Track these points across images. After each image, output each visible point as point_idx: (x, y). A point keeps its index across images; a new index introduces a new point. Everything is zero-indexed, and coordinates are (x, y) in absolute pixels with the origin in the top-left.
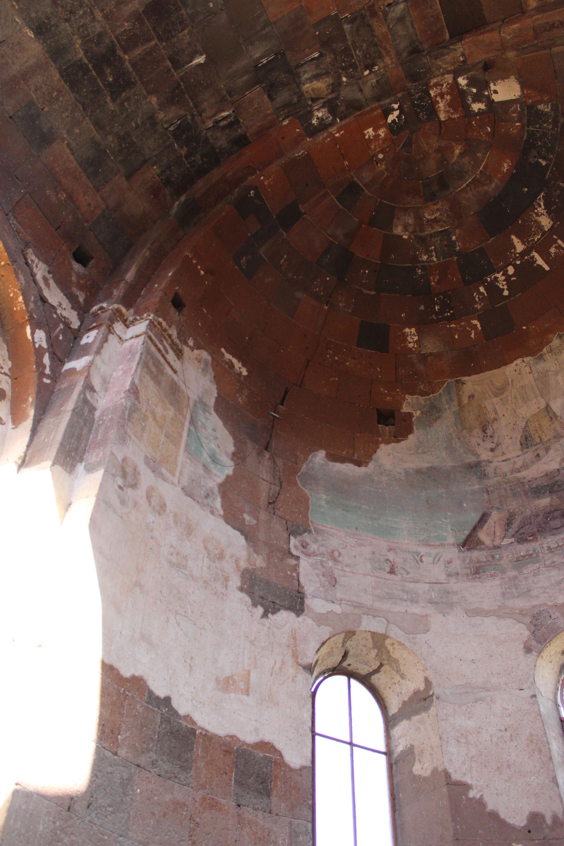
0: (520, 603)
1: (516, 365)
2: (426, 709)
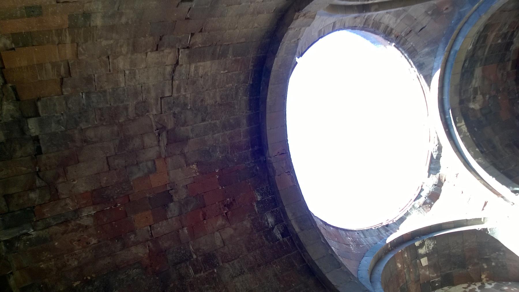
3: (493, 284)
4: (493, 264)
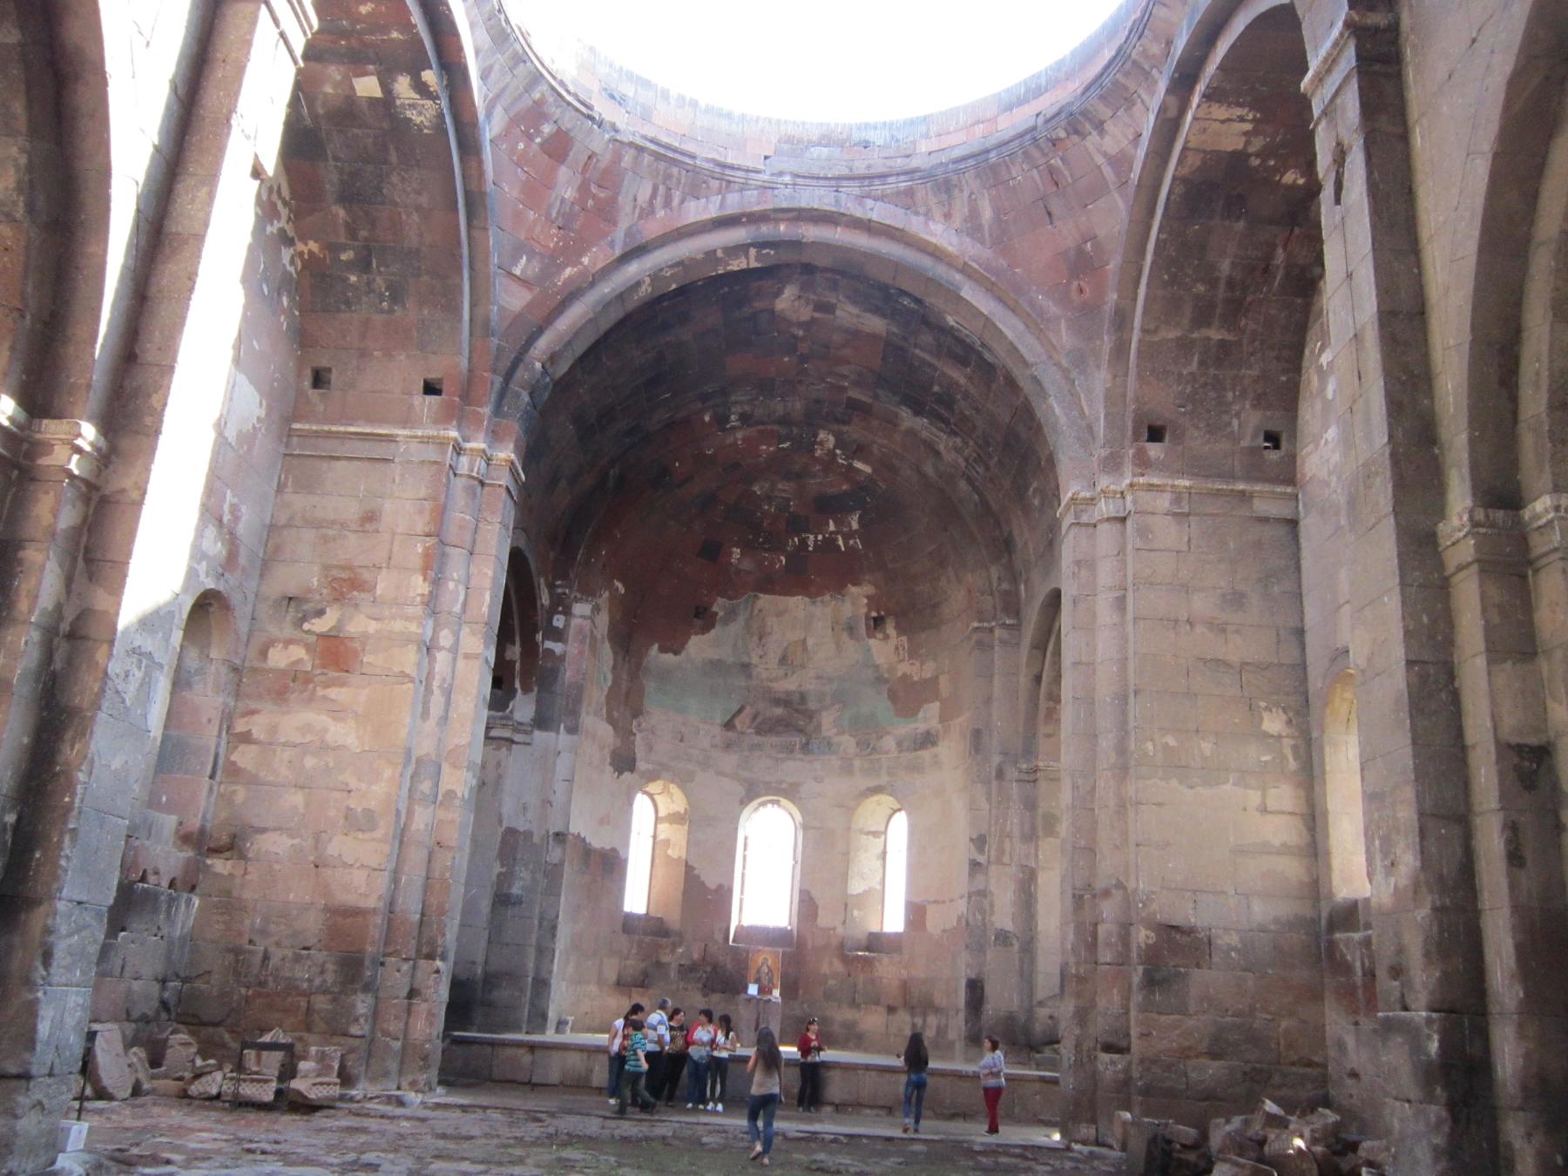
0: (746, 774)
2: (682, 824)
3: (291, 269)
4: (353, 279)
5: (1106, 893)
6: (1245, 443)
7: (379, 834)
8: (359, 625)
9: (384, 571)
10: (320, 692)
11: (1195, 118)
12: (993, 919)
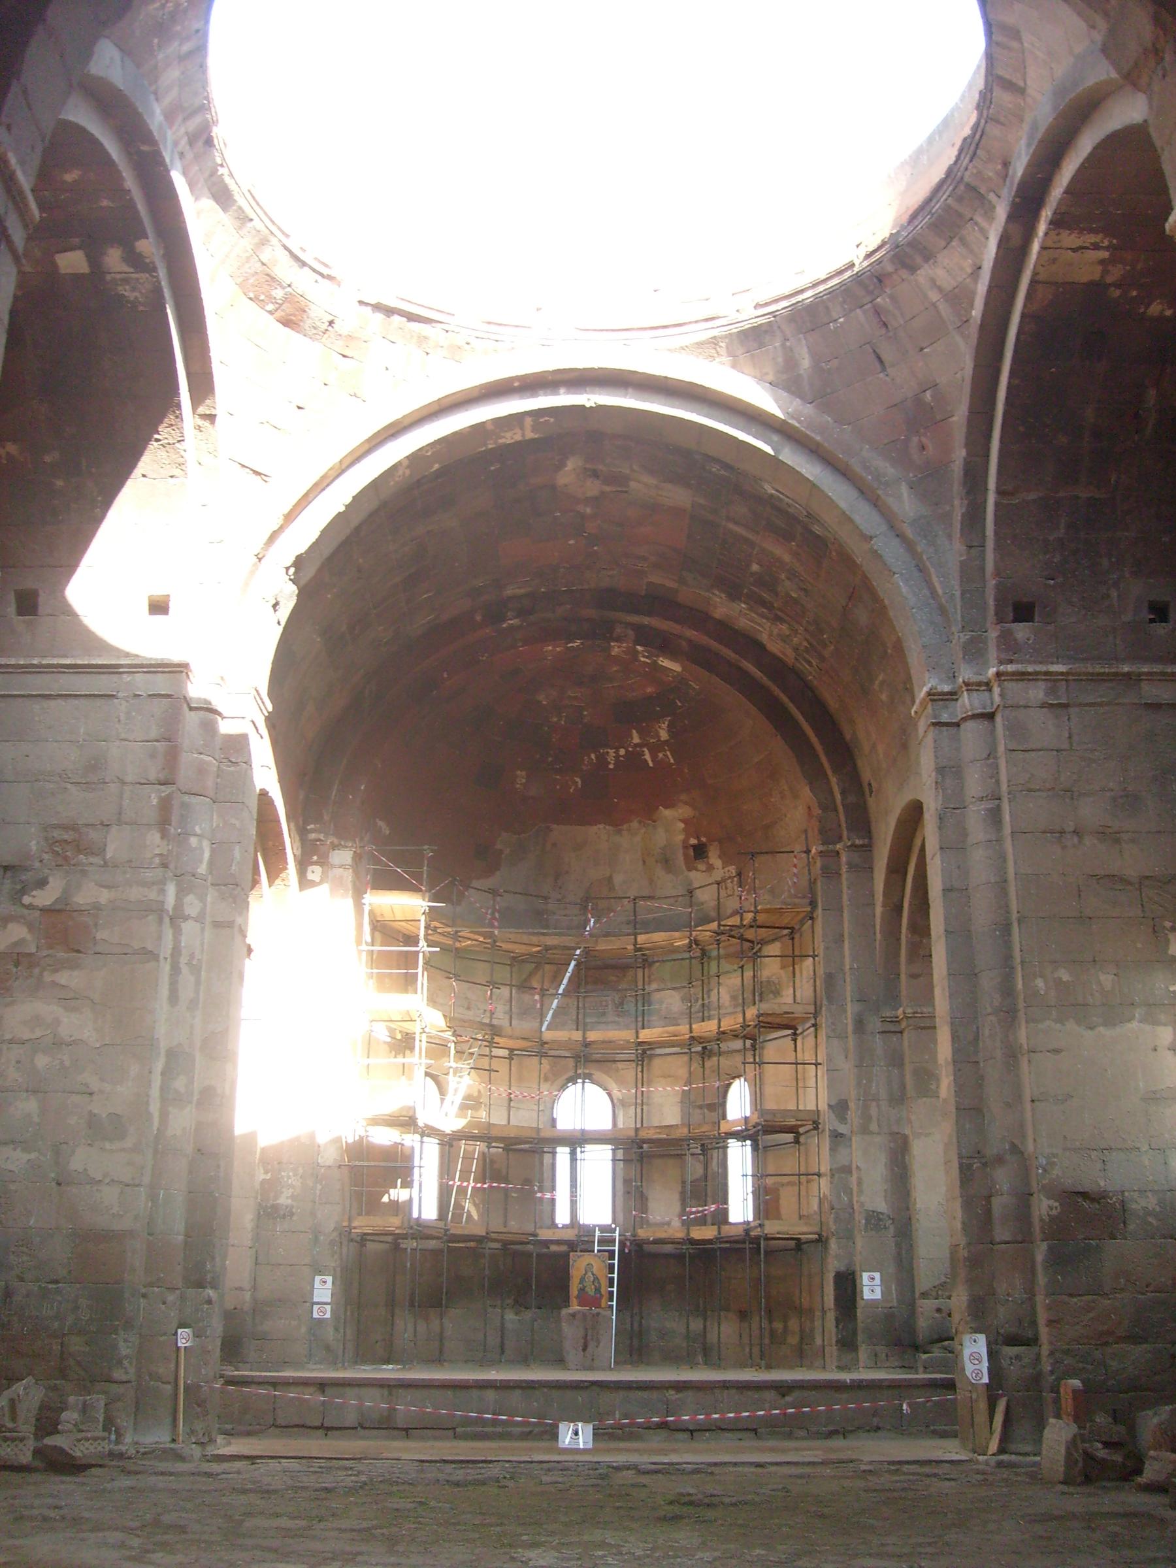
1: (599, 829)
5: (1000, 1160)
6: (1128, 617)
7: (129, 1143)
8: (88, 894)
9: (114, 829)
10: (48, 977)
11: (1043, 248)
12: (862, 1199)
